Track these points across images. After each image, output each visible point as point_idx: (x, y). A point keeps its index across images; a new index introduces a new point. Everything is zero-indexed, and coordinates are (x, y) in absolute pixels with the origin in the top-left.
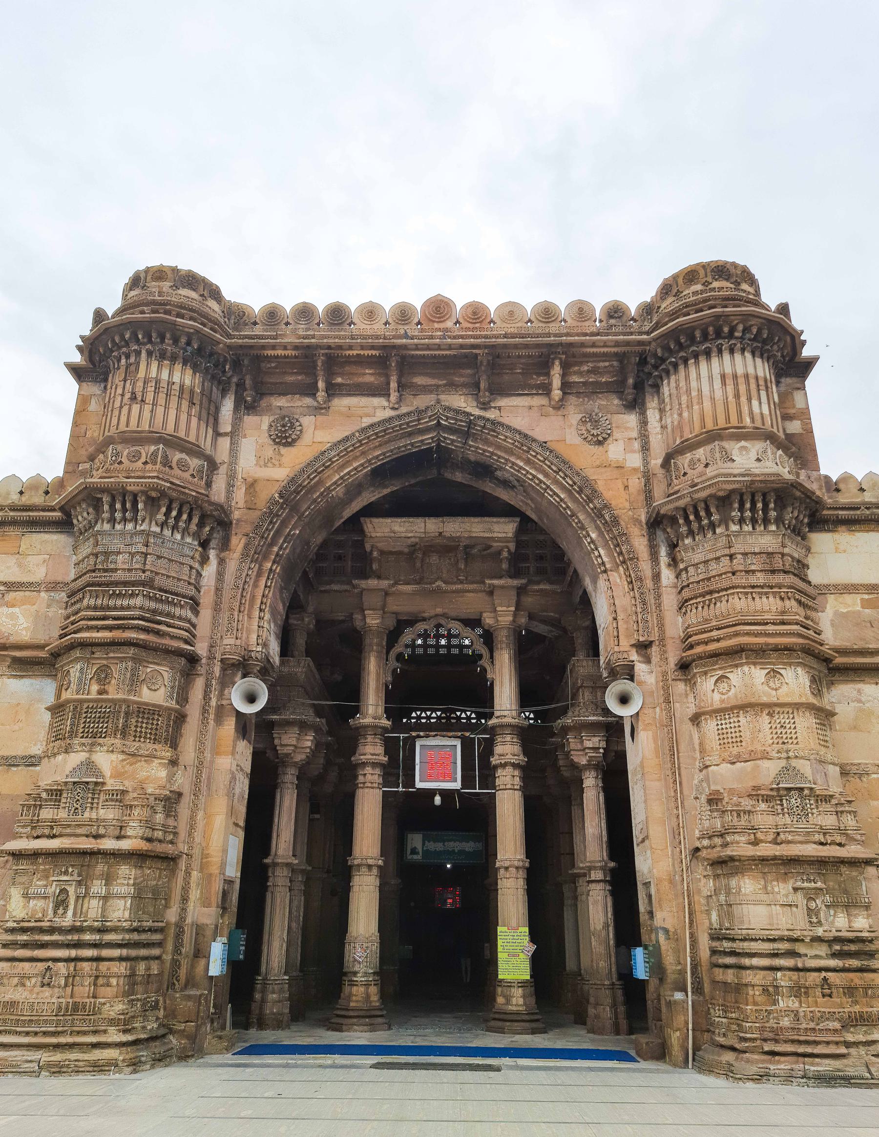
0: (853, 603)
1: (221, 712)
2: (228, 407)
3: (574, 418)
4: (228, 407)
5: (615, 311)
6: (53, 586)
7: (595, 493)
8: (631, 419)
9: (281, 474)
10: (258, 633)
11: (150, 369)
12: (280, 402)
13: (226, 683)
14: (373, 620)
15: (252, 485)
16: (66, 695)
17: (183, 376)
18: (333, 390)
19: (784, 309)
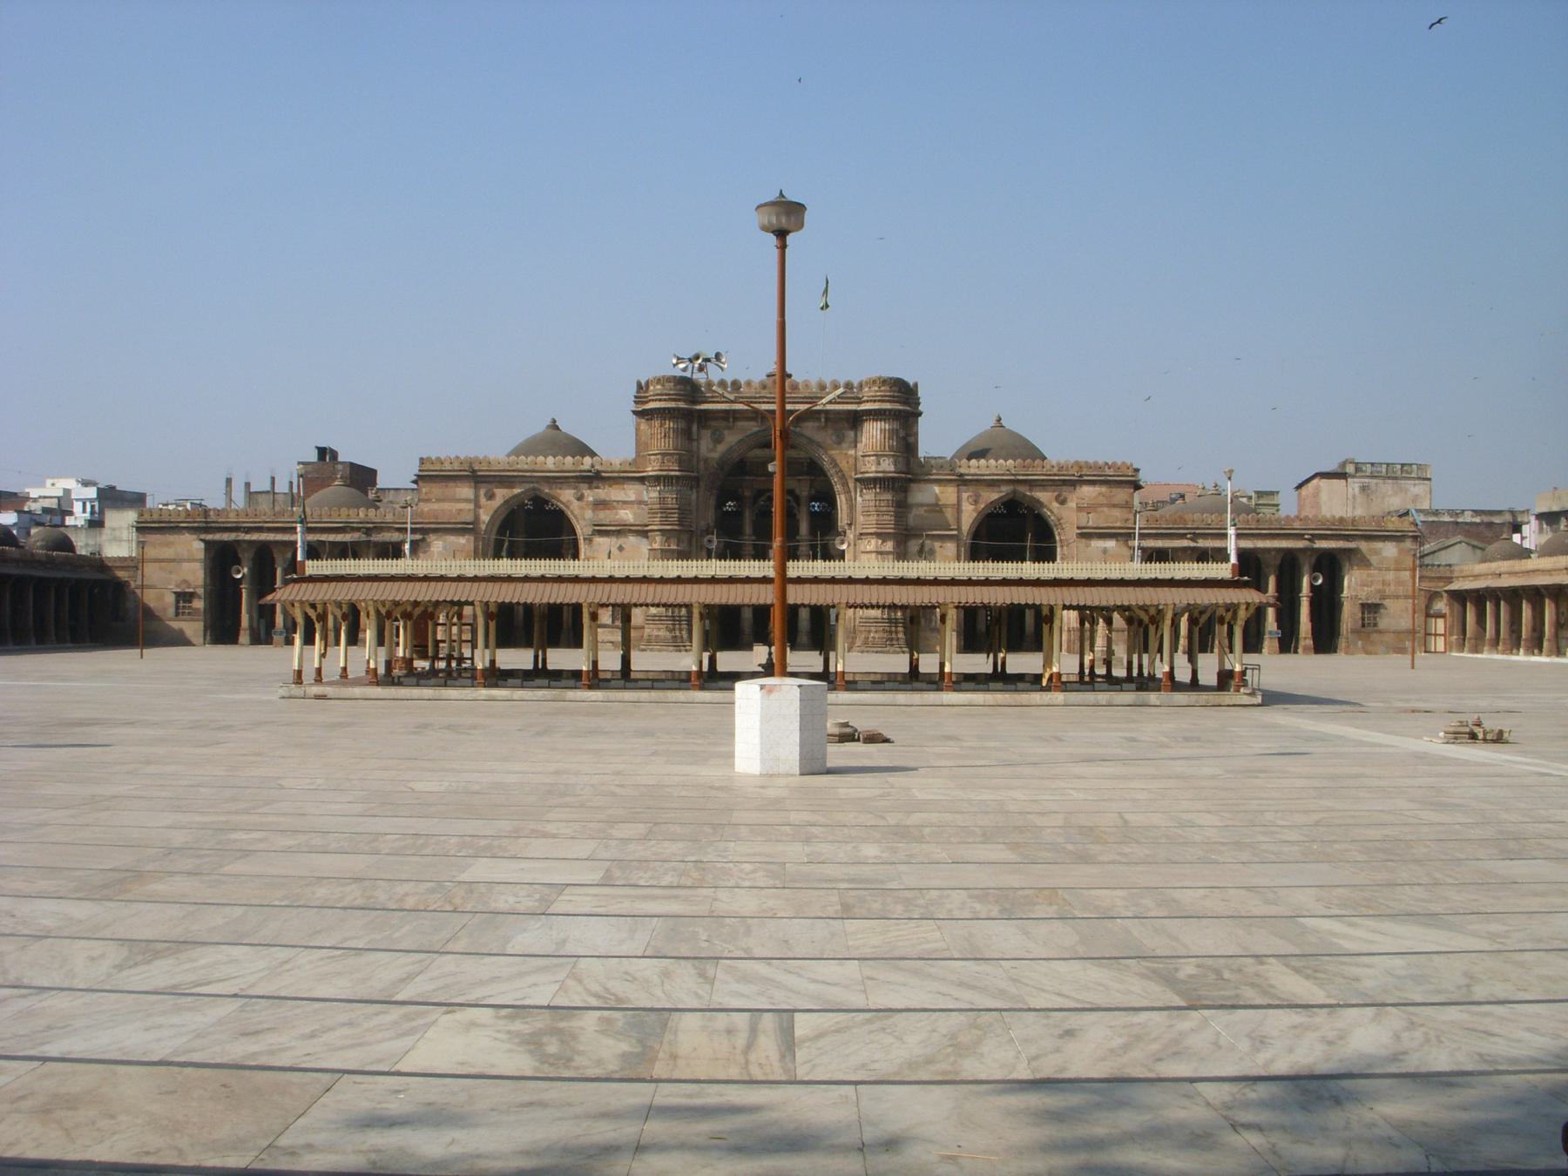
0: (921, 511)
1: (702, 547)
2: (695, 428)
3: (830, 431)
4: (695, 428)
5: (849, 386)
6: (640, 502)
7: (836, 465)
8: (852, 434)
9: (716, 455)
10: (710, 516)
11: (669, 424)
12: (714, 424)
13: (702, 536)
14: (747, 493)
15: (706, 460)
16: (656, 546)
17: (682, 425)
18: (736, 419)
19: (916, 385)
